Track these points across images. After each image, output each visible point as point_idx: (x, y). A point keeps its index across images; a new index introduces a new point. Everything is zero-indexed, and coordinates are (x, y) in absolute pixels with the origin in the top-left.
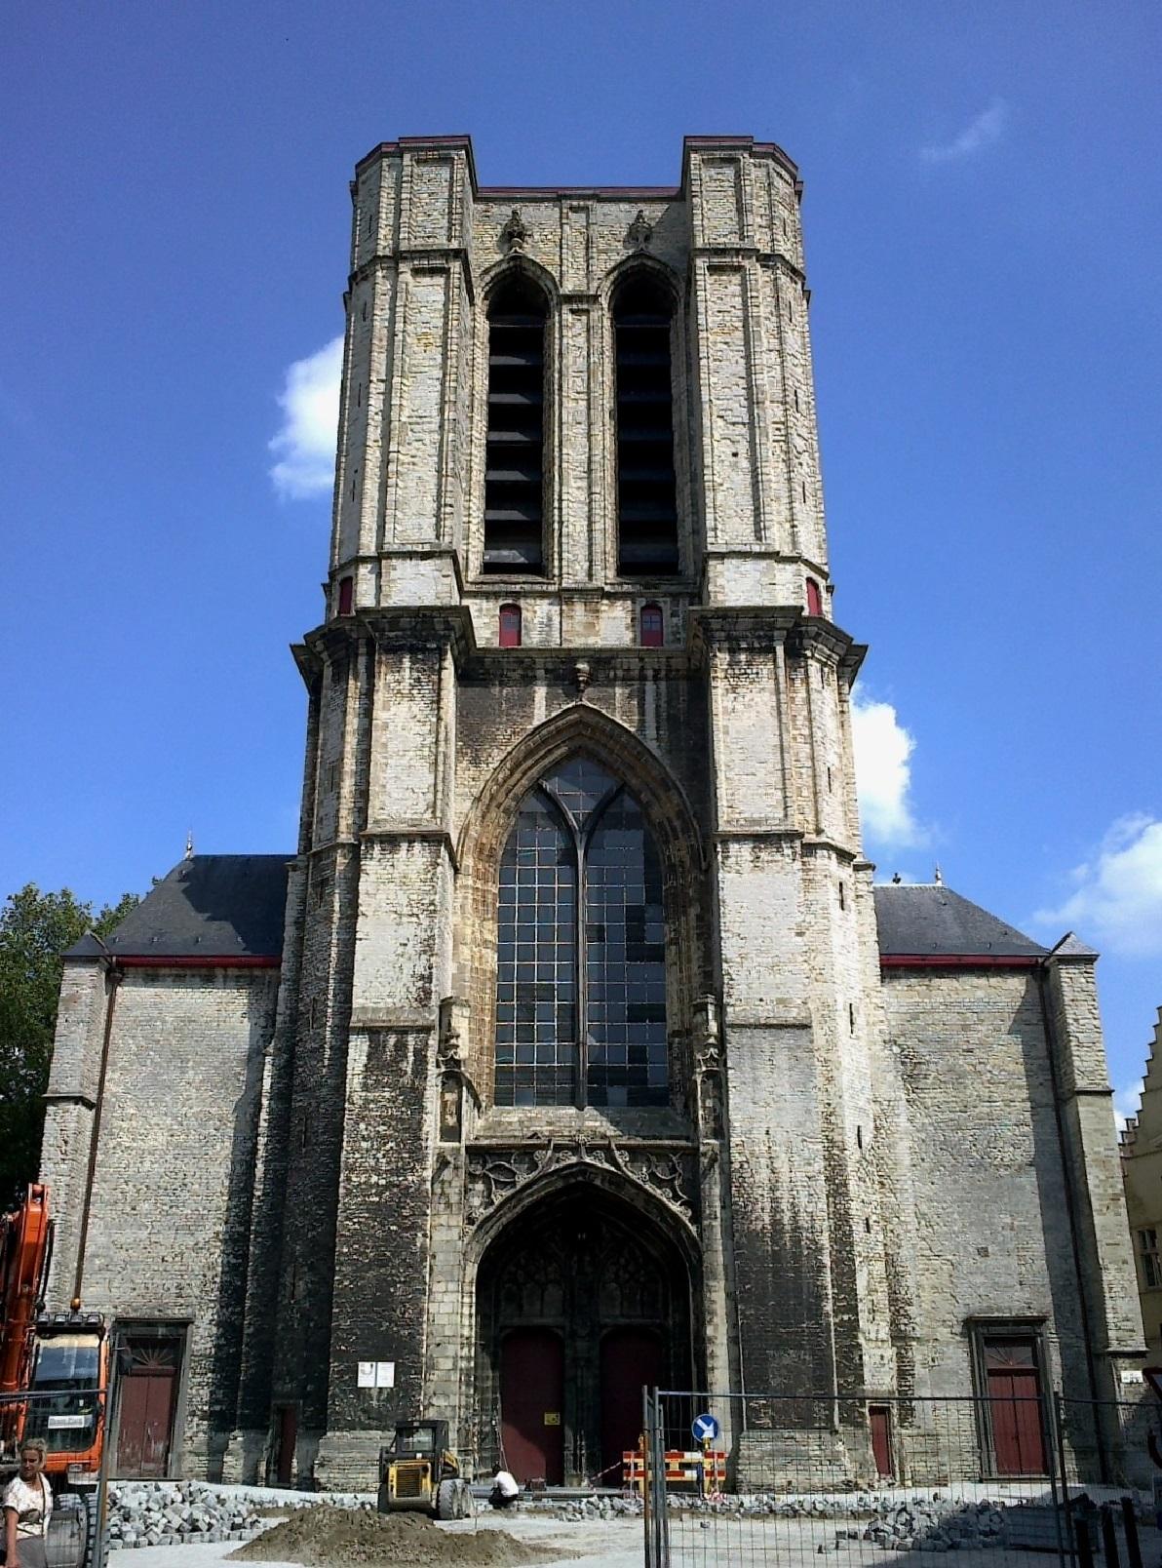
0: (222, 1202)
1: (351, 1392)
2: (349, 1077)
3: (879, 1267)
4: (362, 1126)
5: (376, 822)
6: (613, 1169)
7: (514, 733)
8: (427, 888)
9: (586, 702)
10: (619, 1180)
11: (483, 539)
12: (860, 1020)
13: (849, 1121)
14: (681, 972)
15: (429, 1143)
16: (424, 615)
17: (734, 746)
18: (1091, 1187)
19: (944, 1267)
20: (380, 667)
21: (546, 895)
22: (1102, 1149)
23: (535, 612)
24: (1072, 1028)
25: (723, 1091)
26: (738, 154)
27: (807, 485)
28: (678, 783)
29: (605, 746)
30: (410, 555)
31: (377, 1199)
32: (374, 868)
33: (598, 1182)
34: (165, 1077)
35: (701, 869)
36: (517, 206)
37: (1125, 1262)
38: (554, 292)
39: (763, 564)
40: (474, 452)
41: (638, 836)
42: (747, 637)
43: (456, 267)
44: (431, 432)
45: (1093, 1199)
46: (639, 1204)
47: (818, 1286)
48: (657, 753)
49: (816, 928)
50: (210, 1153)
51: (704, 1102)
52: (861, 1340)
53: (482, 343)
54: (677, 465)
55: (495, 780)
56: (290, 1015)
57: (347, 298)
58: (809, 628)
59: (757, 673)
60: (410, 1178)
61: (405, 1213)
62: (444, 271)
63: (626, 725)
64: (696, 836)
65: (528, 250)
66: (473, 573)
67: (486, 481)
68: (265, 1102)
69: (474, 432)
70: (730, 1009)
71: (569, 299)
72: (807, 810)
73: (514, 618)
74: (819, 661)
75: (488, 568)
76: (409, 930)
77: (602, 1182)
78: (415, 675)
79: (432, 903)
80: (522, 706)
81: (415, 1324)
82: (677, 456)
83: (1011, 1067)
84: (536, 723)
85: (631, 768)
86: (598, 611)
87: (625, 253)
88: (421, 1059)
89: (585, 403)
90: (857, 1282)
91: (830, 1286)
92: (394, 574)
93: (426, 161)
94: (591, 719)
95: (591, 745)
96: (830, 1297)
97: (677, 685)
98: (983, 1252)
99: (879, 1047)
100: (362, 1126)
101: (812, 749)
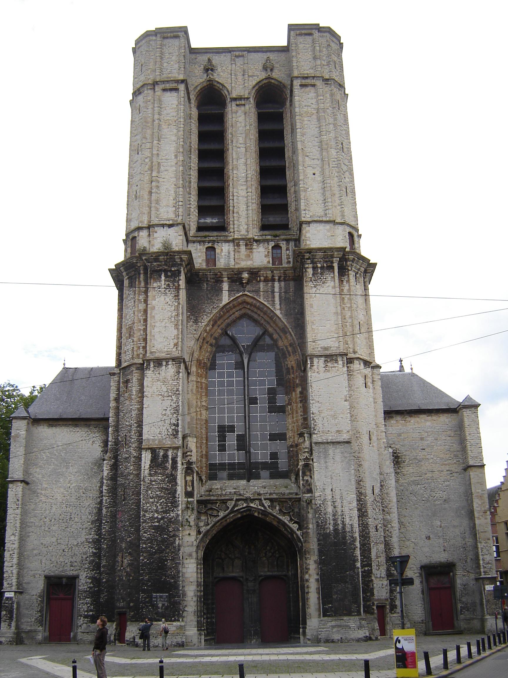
0: (88, 525)
1: (150, 606)
2: (142, 470)
3: (382, 547)
4: (150, 492)
5: (151, 353)
6: (263, 508)
7: (213, 308)
8: (175, 383)
9: (246, 293)
10: (265, 513)
11: (197, 215)
12: (374, 438)
13: (368, 484)
14: (293, 418)
15: (180, 499)
16: (171, 255)
17: (315, 313)
18: (475, 508)
19: (411, 545)
20: (151, 280)
21: (230, 384)
22: (480, 491)
23: (222, 250)
24: (468, 438)
25: (312, 472)
26: (313, 31)
27: (348, 187)
28: (290, 329)
29: (256, 313)
30: (163, 226)
31: (157, 524)
32: (150, 374)
33: (256, 514)
34: (60, 471)
35: (301, 369)
37: (489, 539)
38: (228, 97)
39: (328, 226)
40: (192, 173)
41: (272, 355)
42: (321, 261)
43: (182, 87)
44: (172, 166)
45: (475, 513)
46: (275, 523)
47: (354, 556)
48: (280, 316)
49: (354, 397)
50: (82, 504)
51: (303, 477)
52: (373, 578)
53: (195, 121)
54: (287, 177)
55: (205, 331)
56: (115, 442)
58: (350, 257)
59: (326, 278)
60: (172, 515)
61: (170, 529)
62: (176, 90)
63: (266, 303)
64: (299, 354)
66: (193, 231)
67: (198, 187)
68: (105, 481)
69: (191, 164)
70: (314, 436)
71: (235, 99)
72: (349, 342)
73: (213, 253)
74: (354, 271)
75: (200, 228)
76: (168, 403)
77: (258, 514)
78: (167, 283)
79: (178, 390)
80: (217, 295)
81: (176, 577)
82: (288, 173)
83: (442, 456)
85: (269, 323)
86: (251, 249)
87: (263, 75)
88: (174, 462)
89: (244, 149)
90: (372, 554)
91: (359, 556)
92: (156, 235)
93: (167, 38)
94: (249, 300)
95: (249, 312)
96: (359, 560)
97: (289, 284)
98: (428, 538)
99: (383, 449)
100: (150, 492)
101: (352, 313)
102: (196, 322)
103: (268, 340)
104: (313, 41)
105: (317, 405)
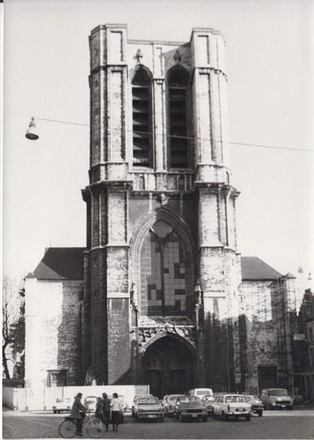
41: (176, 244)
57: (91, 77)
65: (143, 61)
102: (134, 223)
103: (175, 235)
105: (205, 275)
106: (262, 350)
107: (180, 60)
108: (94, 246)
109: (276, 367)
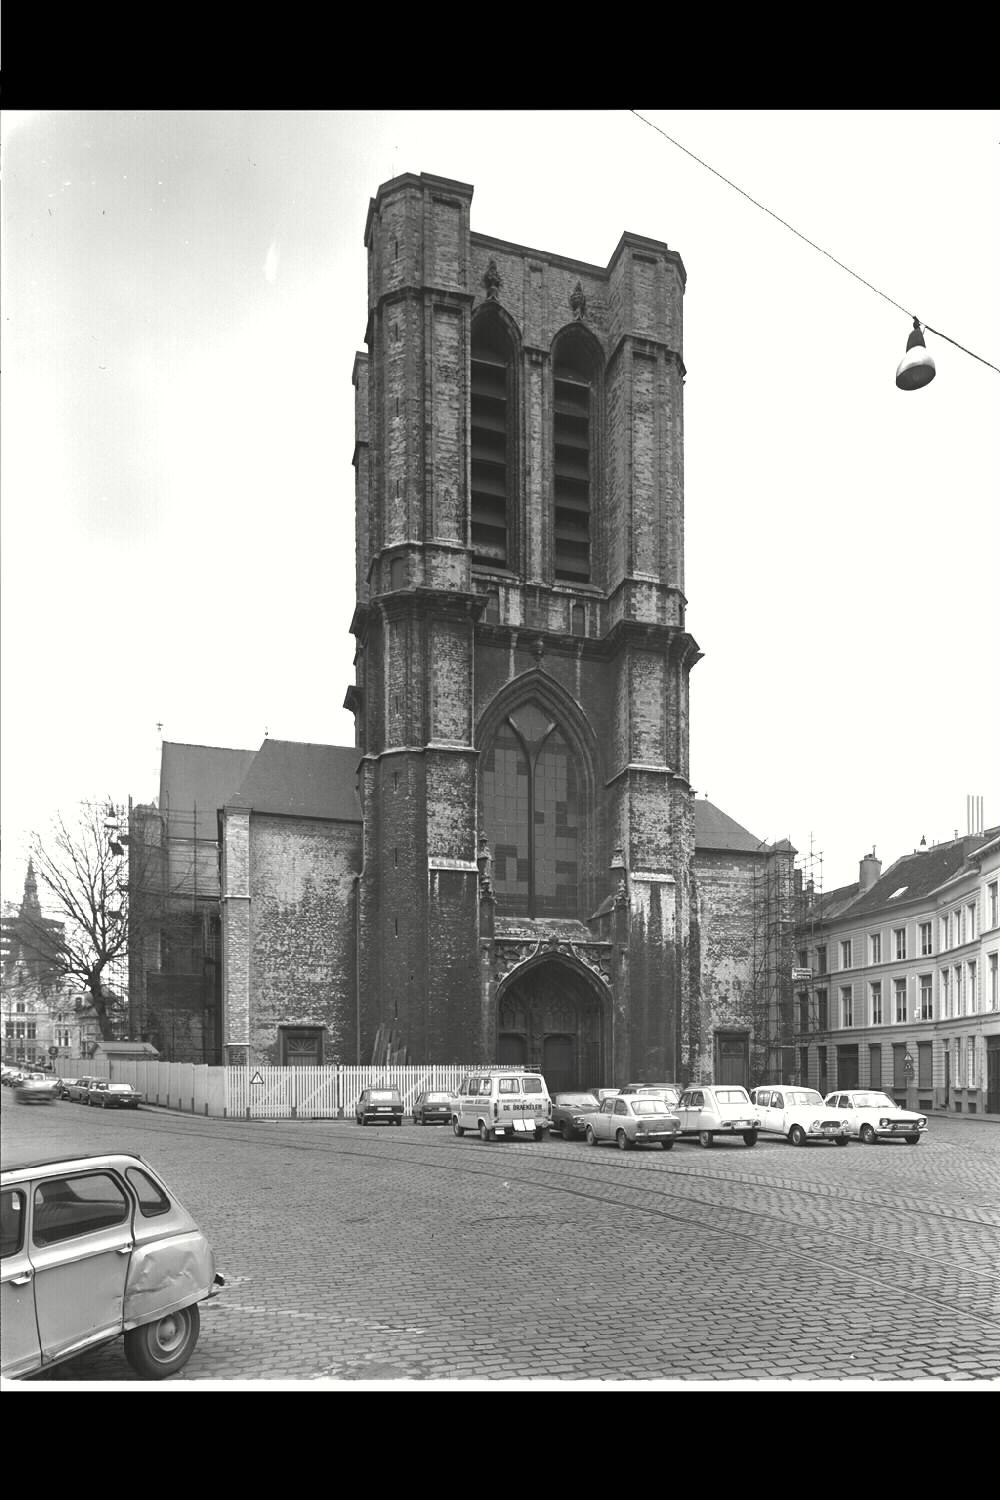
36: (491, 253)
84: (512, 678)
104: (658, 279)
106: (724, 999)
107: (583, 311)
108: (391, 746)
109: (748, 1033)
